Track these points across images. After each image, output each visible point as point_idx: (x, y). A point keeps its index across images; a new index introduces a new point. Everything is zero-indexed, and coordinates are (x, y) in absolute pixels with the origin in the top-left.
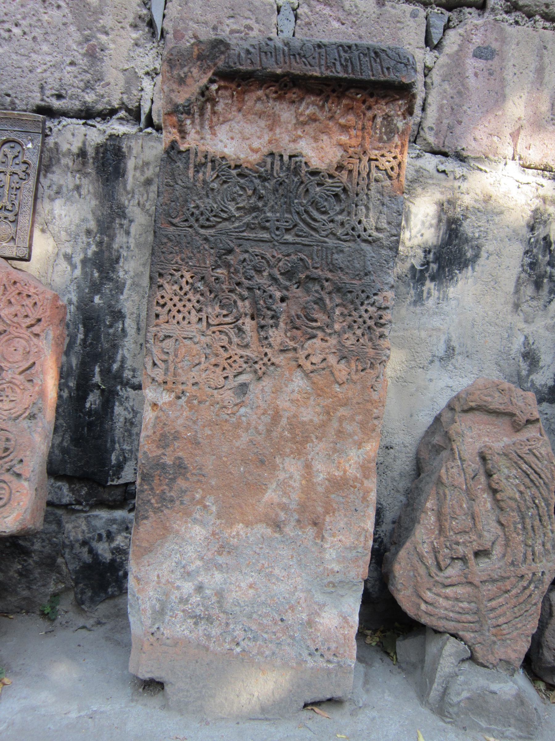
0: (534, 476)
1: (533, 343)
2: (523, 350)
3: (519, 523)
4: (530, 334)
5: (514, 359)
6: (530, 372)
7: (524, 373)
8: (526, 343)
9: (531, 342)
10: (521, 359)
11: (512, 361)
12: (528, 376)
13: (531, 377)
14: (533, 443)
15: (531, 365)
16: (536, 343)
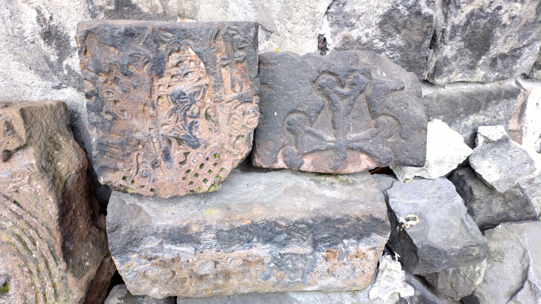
0: (27, 217)
1: (51, 18)
2: (40, 29)
3: (24, 266)
4: (42, 6)
5: (33, 43)
6: (62, 57)
7: (54, 58)
8: (41, 19)
9: (47, 16)
10: (42, 42)
11: (32, 46)
12: (60, 61)
13: (65, 63)
14: (18, 179)
15: (58, 47)
16: (55, 17)
